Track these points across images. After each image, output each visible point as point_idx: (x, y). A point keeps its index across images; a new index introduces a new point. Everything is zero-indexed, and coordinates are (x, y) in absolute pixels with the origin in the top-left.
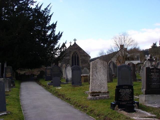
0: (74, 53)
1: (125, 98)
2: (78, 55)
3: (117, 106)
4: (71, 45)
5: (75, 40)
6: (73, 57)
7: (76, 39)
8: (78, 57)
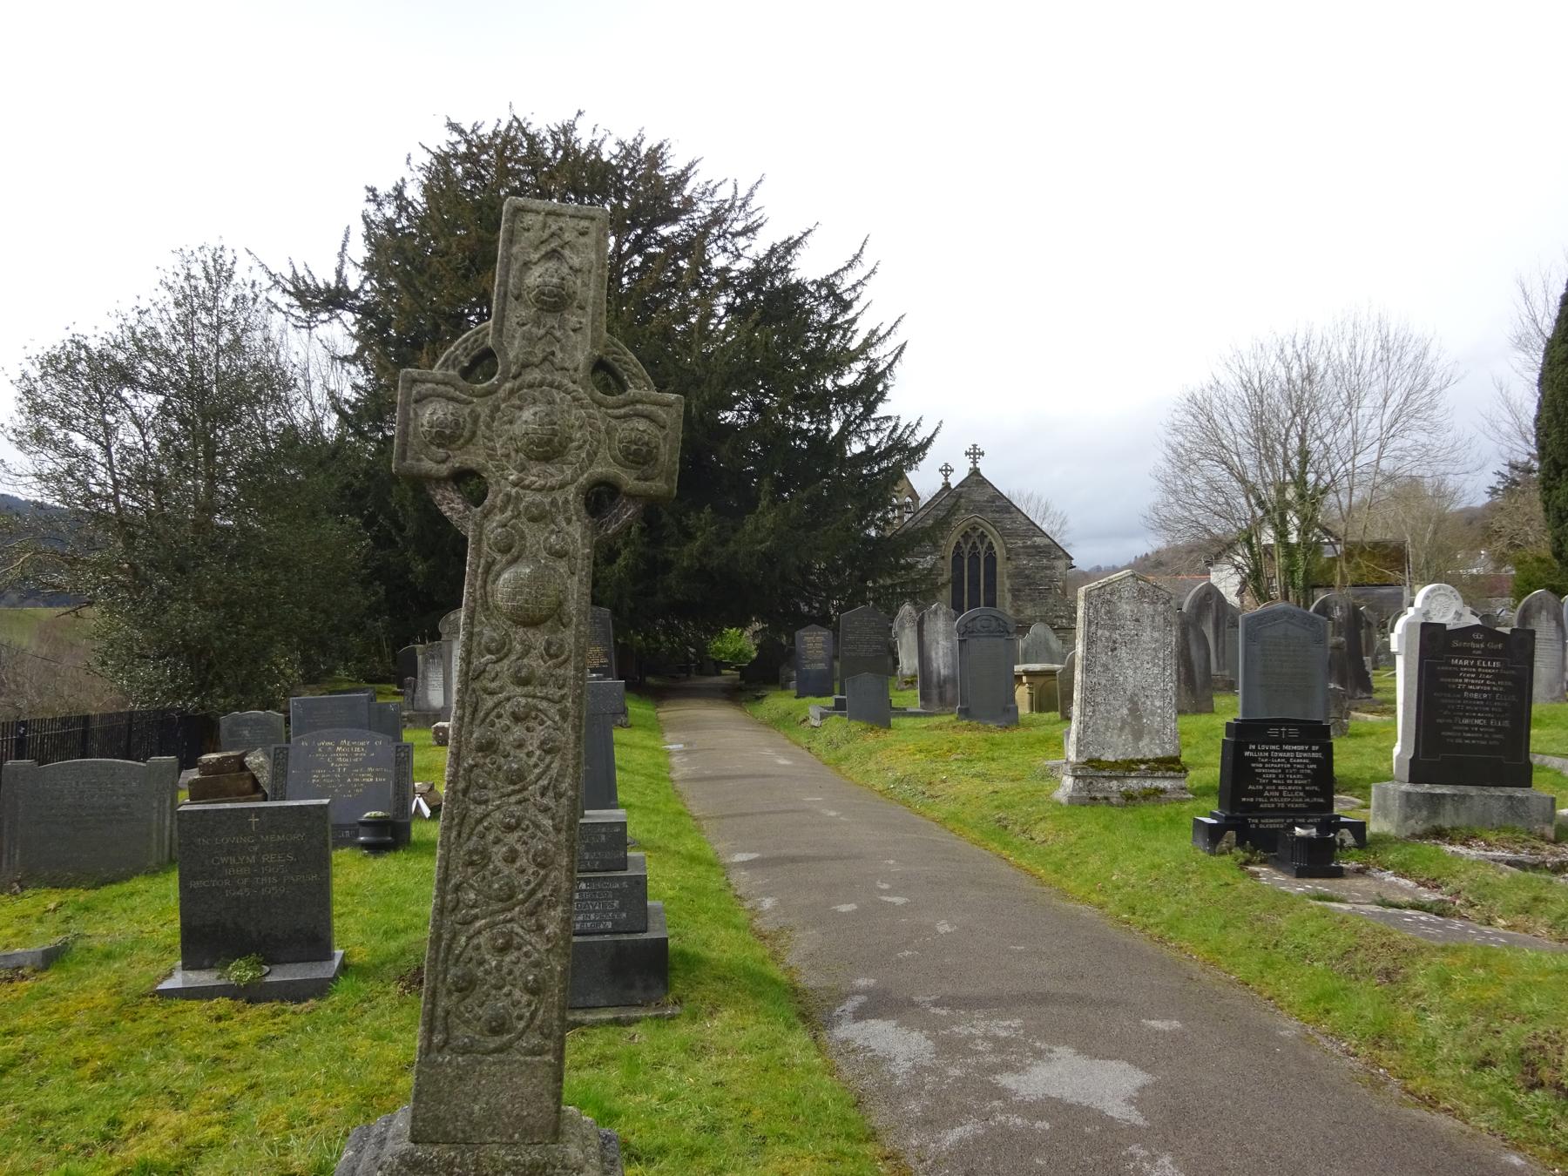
0: (966, 536)
1: (1281, 796)
2: (990, 546)
3: (1231, 835)
4: (947, 486)
6: (958, 557)
8: (991, 560)
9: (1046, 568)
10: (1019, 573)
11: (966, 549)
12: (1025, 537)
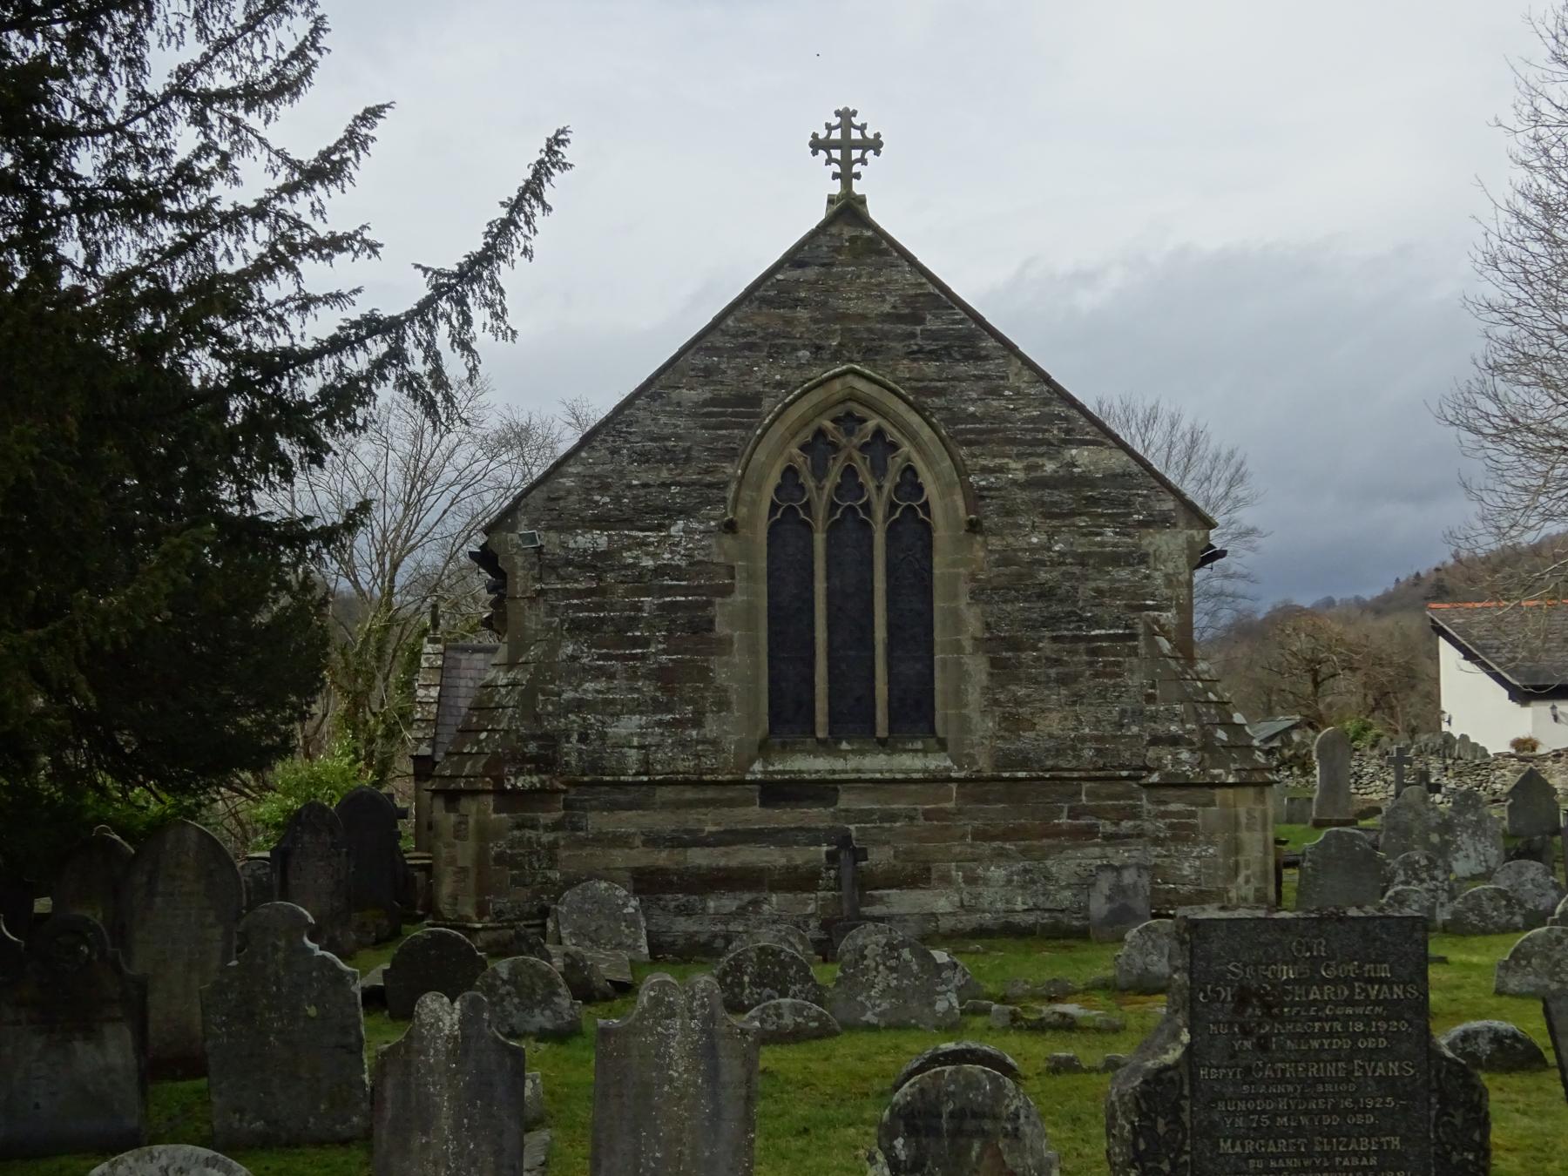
0: (818, 446)
2: (910, 483)
5: (846, 144)
6: (788, 521)
7: (871, 120)
8: (912, 529)
9: (1116, 559)
10: (1009, 581)
11: (820, 493)
12: (1034, 444)
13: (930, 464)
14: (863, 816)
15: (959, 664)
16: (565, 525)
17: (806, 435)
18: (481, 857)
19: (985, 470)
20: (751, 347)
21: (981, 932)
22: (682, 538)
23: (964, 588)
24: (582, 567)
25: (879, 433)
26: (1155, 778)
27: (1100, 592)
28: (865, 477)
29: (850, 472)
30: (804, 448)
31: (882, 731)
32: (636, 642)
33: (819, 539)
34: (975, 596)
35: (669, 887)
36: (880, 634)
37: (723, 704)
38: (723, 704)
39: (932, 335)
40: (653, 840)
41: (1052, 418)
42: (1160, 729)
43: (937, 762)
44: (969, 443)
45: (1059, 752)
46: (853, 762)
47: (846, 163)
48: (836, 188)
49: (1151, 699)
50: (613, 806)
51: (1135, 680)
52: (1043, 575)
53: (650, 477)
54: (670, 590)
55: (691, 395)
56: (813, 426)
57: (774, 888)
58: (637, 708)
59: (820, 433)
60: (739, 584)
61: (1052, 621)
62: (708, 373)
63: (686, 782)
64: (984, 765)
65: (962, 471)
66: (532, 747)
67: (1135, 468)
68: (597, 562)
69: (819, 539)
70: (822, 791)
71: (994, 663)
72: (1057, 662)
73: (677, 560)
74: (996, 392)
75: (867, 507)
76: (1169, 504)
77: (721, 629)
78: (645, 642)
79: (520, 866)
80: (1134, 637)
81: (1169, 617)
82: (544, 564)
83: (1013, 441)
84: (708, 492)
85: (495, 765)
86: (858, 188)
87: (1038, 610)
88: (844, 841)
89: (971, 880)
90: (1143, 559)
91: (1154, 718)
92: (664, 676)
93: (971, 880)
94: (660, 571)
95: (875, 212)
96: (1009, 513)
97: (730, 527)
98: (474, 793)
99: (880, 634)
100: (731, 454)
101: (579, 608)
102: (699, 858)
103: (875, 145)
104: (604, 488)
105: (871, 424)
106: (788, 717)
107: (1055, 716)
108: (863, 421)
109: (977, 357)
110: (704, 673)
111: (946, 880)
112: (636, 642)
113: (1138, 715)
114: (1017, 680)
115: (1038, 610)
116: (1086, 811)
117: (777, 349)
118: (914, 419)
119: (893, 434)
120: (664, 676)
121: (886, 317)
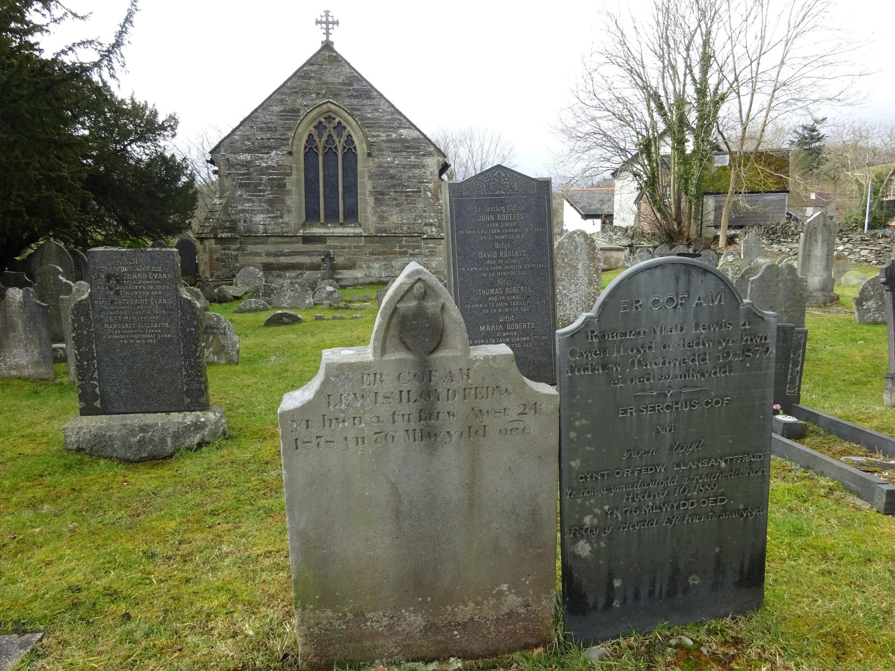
0: (320, 127)
2: (349, 140)
5: (327, 23)
6: (310, 152)
7: (335, 15)
9: (414, 166)
10: (382, 173)
12: (389, 128)
13: (356, 134)
14: (335, 247)
15: (365, 199)
16: (235, 151)
17: (315, 123)
18: (211, 258)
19: (373, 136)
20: (296, 93)
21: (372, 284)
22: (275, 157)
23: (366, 175)
24: (242, 166)
25: (339, 123)
26: (425, 236)
27: (409, 177)
28: (335, 138)
29: (330, 136)
30: (315, 127)
31: (341, 221)
32: (261, 191)
33: (321, 158)
34: (370, 177)
35: (274, 269)
36: (340, 189)
37: (289, 211)
38: (289, 211)
39: (356, 90)
40: (268, 254)
41: (394, 119)
42: (427, 221)
43: (358, 231)
44: (368, 127)
45: (396, 228)
46: (332, 230)
47: (327, 29)
48: (324, 38)
49: (425, 211)
50: (256, 243)
51: (420, 206)
52: (391, 171)
53: (264, 136)
54: (271, 174)
55: (277, 109)
56: (318, 121)
57: (307, 269)
58: (262, 212)
59: (320, 122)
60: (294, 172)
61: (394, 186)
62: (282, 101)
63: (278, 236)
64: (373, 232)
65: (366, 137)
66: (227, 224)
67: (421, 137)
68: (247, 164)
69: (321, 158)
70: (321, 239)
71: (376, 199)
72: (396, 199)
73: (273, 164)
74: (376, 110)
75: (336, 148)
76: (432, 149)
77: (288, 187)
78: (264, 191)
79: (225, 262)
80: (420, 192)
81: (431, 185)
82: (230, 165)
83: (382, 127)
84: (283, 141)
85: (214, 229)
86: (331, 38)
87: (390, 182)
88: (328, 255)
89: (368, 267)
90: (423, 166)
91: (425, 218)
92: (270, 202)
93: (368, 267)
94: (268, 168)
95: (337, 47)
96: (381, 151)
97: (290, 153)
98: (207, 238)
99: (340, 189)
100: (290, 129)
101: (242, 179)
102: (283, 260)
103: (336, 23)
104: (249, 140)
105: (337, 120)
106: (312, 215)
107: (395, 217)
108: (334, 119)
109: (371, 98)
110: (283, 201)
111: (361, 267)
112: (261, 191)
113: (421, 217)
114: (383, 205)
115: (390, 182)
116: (404, 246)
117: (305, 93)
118: (350, 118)
119: (344, 124)
120: (270, 202)
121: (341, 84)
